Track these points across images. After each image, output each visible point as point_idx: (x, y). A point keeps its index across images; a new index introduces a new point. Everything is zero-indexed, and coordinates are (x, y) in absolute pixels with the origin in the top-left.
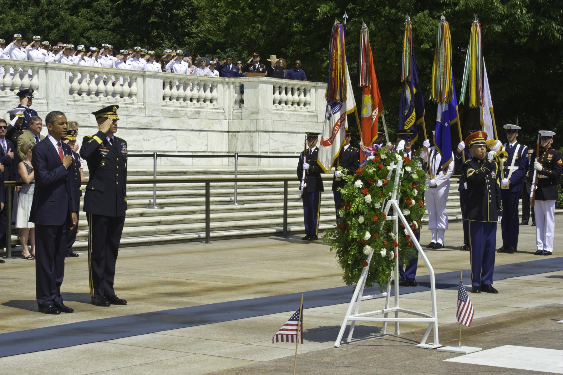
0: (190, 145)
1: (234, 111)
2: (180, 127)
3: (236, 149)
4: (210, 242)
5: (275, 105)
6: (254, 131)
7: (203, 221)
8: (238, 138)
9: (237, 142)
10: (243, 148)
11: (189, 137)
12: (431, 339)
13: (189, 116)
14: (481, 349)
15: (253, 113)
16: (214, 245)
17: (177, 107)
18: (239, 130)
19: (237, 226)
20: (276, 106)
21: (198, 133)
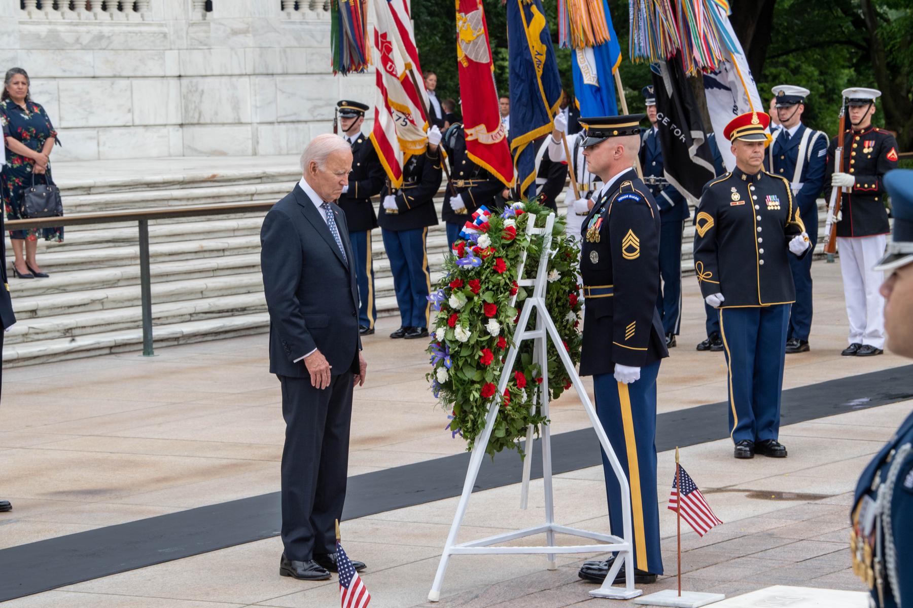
0: (91, 113)
1: (192, 29)
2: (64, 71)
3: (200, 117)
4: (153, 353)
5: (286, 10)
6: (241, 75)
7: (136, 303)
8: (203, 91)
9: (201, 101)
10: (216, 114)
11: (88, 93)
12: (620, 580)
13: (84, 43)
14: (722, 596)
15: (235, 33)
16: (164, 357)
17: (55, 23)
18: (204, 74)
19: (212, 309)
20: (289, 14)
21: (107, 82)
